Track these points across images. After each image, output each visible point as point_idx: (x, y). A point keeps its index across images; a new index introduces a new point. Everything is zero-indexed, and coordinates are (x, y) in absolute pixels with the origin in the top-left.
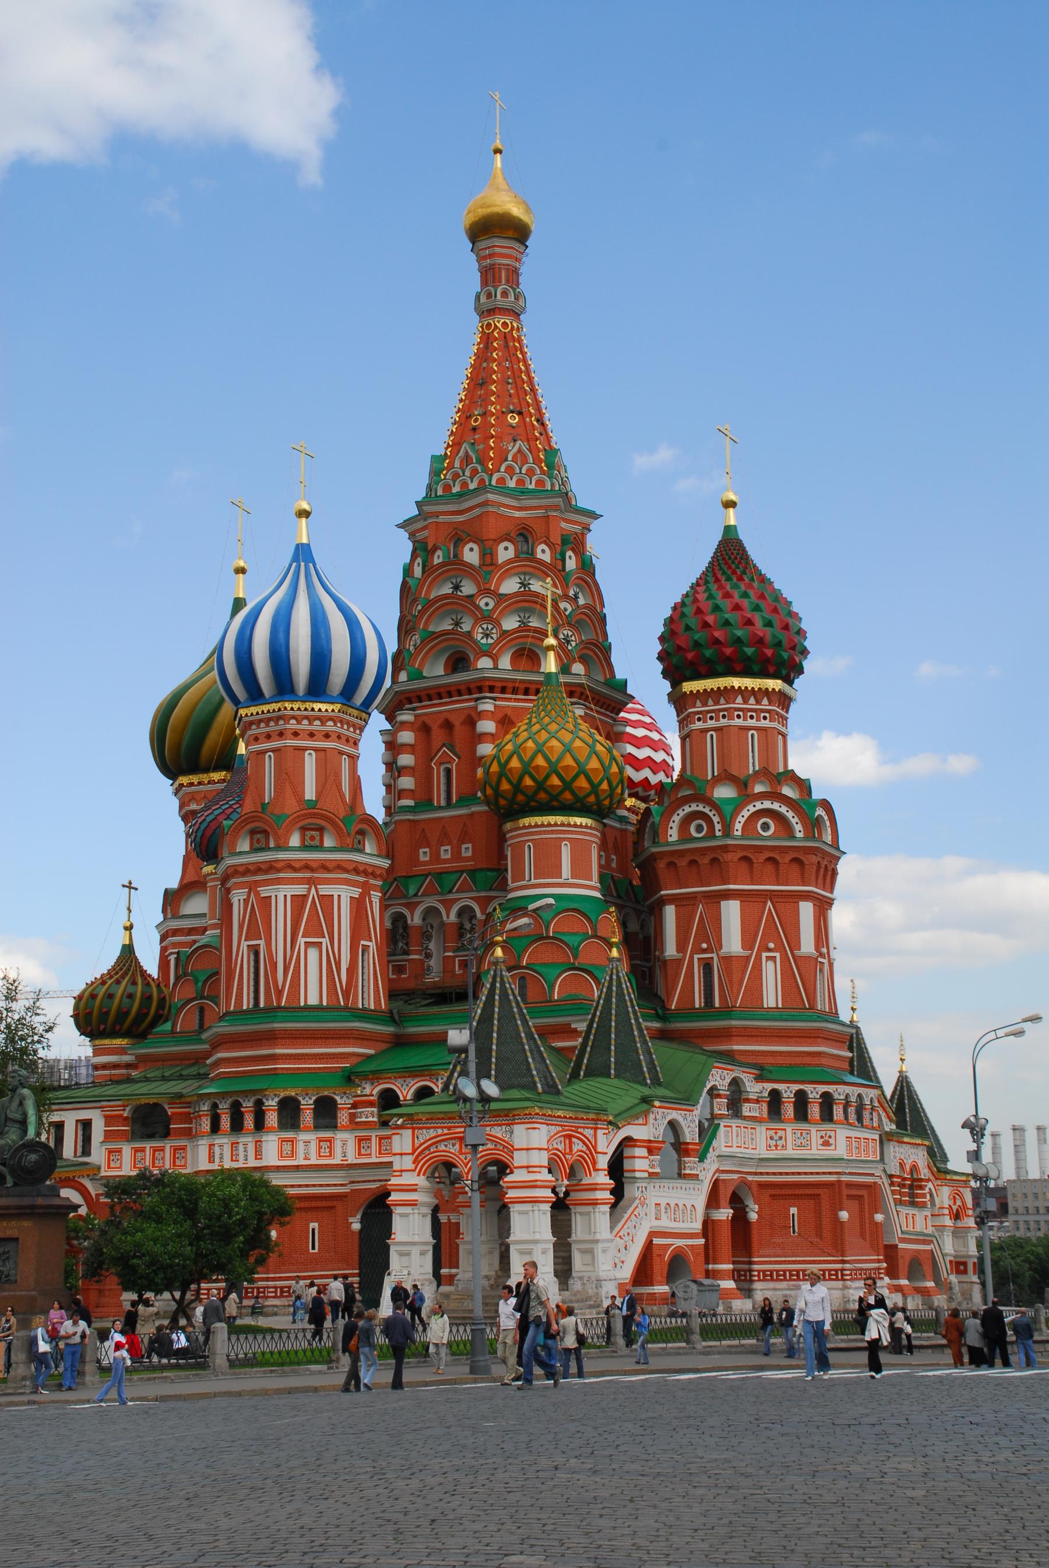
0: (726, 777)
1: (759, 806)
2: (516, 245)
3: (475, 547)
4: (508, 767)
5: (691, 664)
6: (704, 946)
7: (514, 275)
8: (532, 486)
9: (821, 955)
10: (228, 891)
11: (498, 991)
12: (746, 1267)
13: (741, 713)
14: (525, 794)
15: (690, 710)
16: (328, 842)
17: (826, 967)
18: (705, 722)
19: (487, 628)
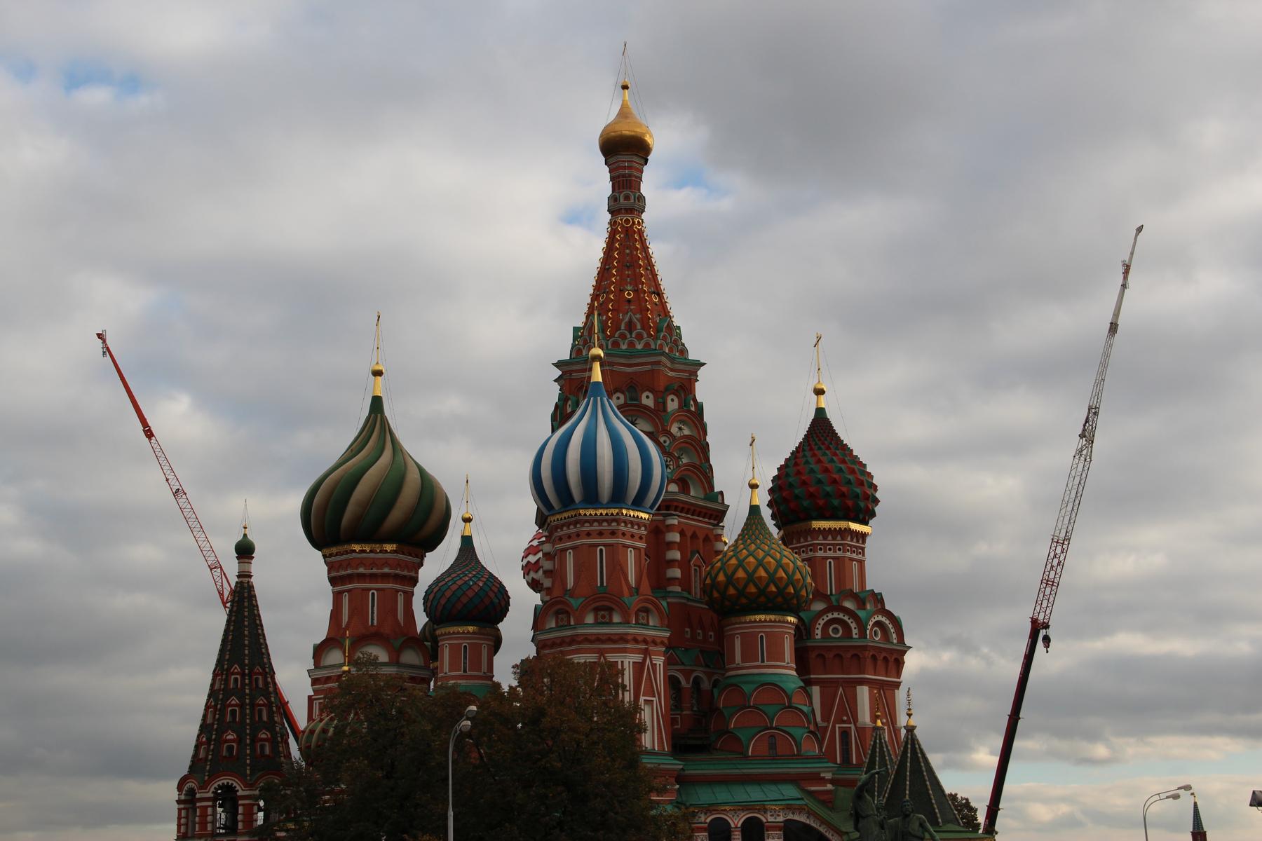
1: (877, 619)
2: (642, 162)
3: (651, 396)
4: (756, 575)
6: (845, 718)
11: (919, 751)
13: (849, 548)
15: (815, 542)
16: (651, 623)
18: (825, 551)
19: (667, 460)
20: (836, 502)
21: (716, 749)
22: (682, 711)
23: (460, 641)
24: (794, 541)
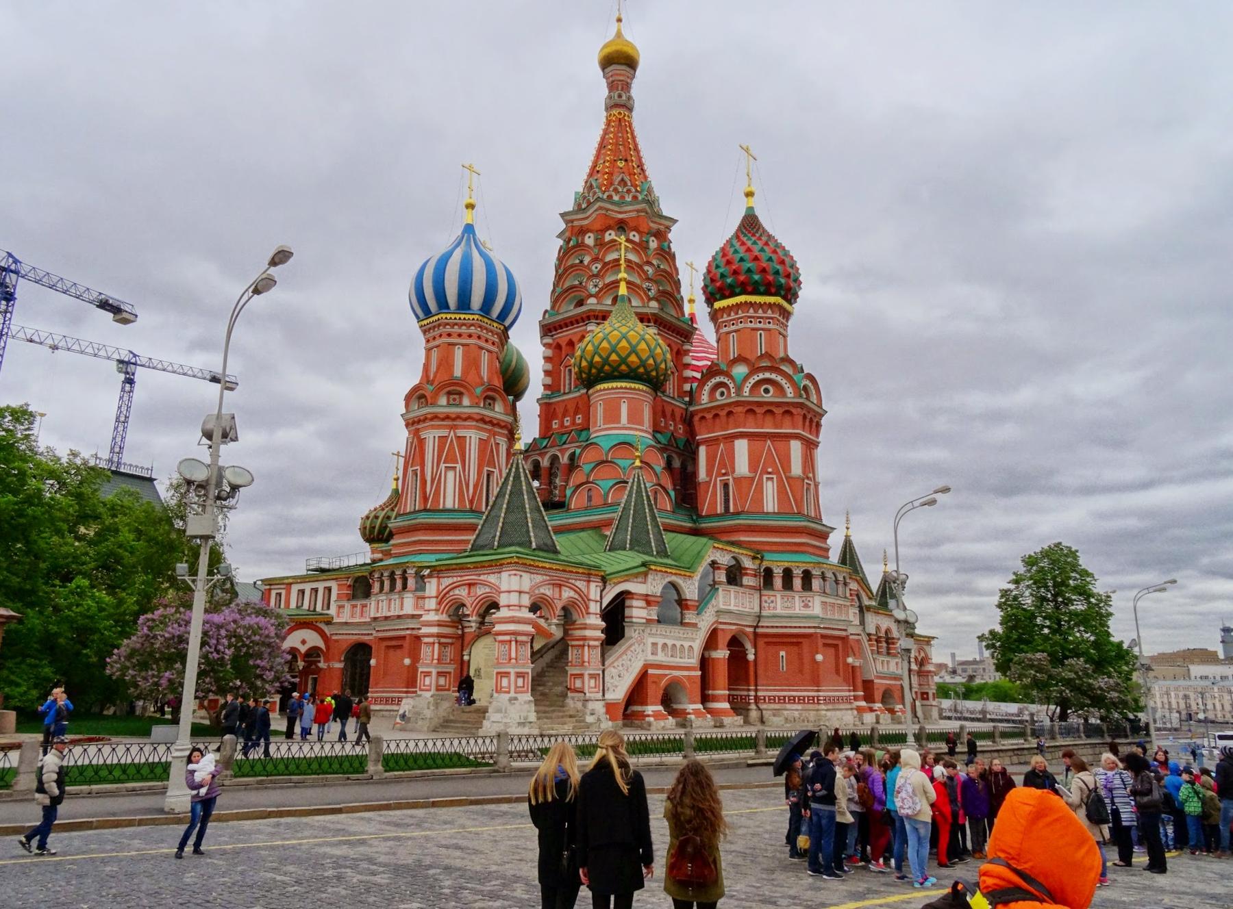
0: (740, 359)
1: (761, 376)
2: (628, 69)
5: (720, 289)
6: (723, 471)
7: (627, 87)
9: (808, 478)
12: (745, 693)
14: (595, 368)
17: (812, 487)
20: (729, 280)
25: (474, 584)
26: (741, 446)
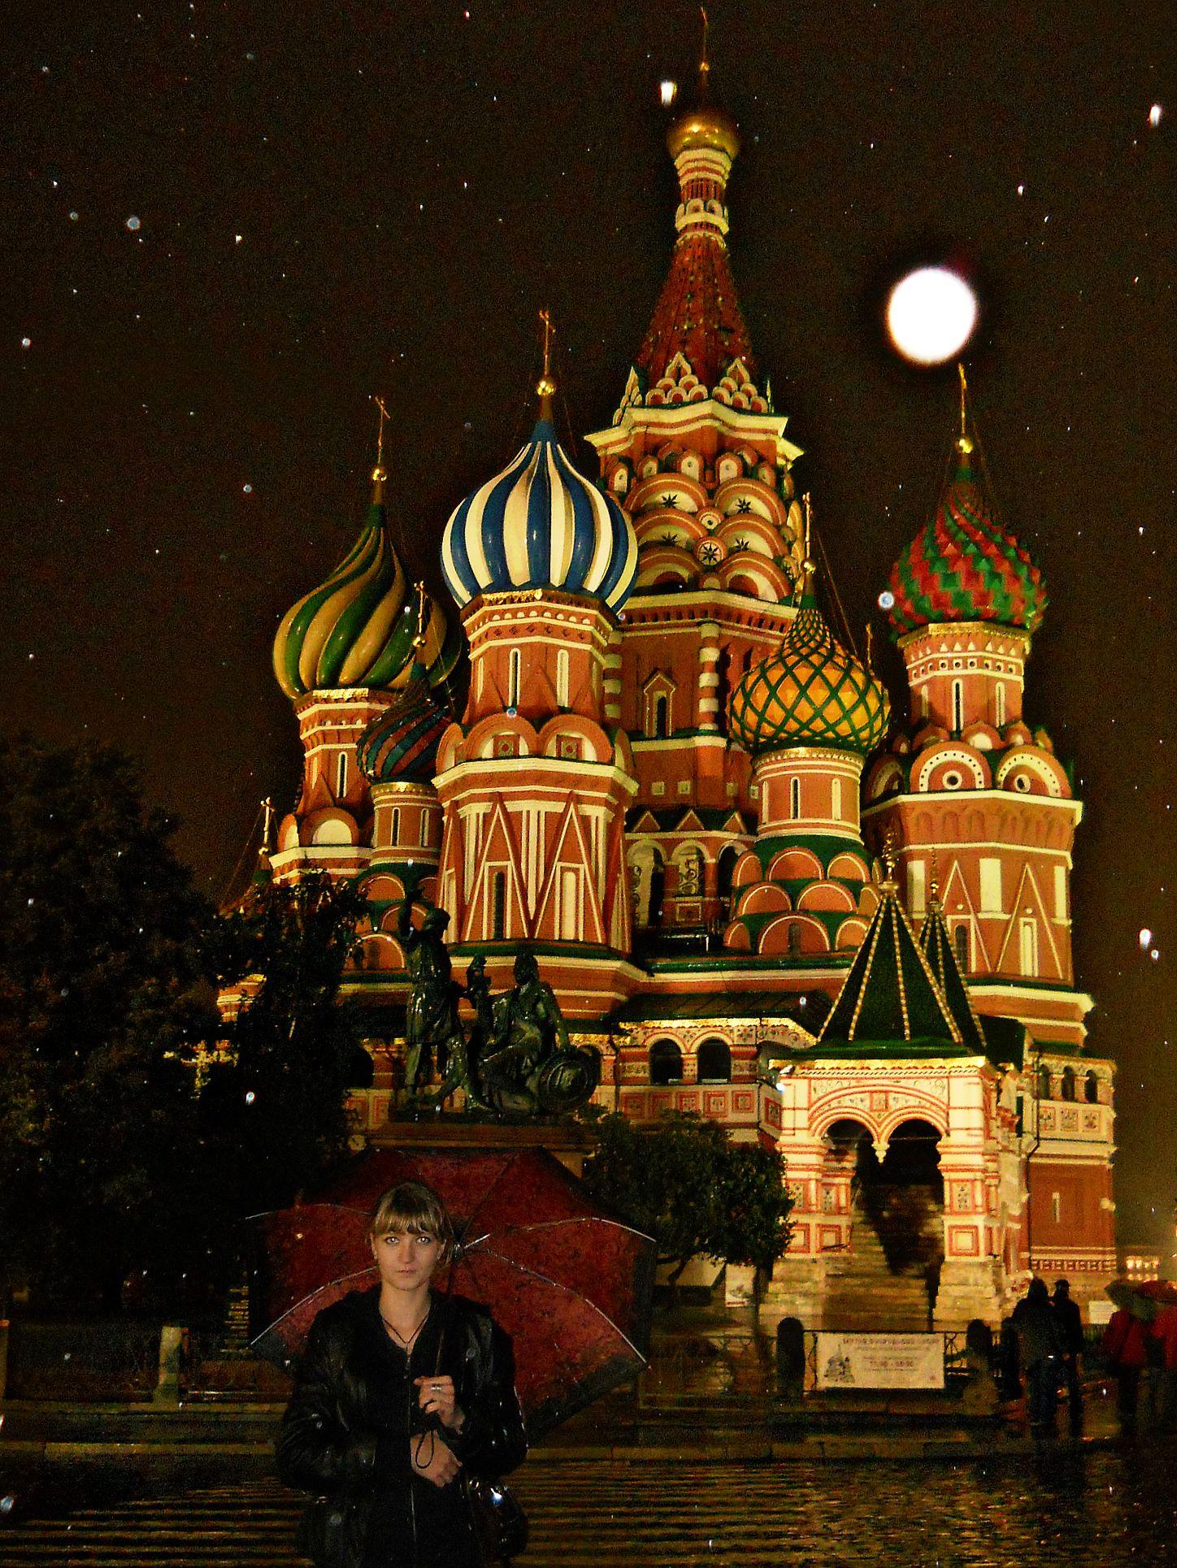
6: (960, 907)
8: (749, 408)
10: (456, 805)
11: (895, 922)
14: (796, 720)
15: (935, 656)
18: (951, 668)
19: (710, 549)
21: (726, 948)
22: (704, 896)
23: (391, 805)
24: (913, 659)
25: (886, 1092)
26: (990, 872)
